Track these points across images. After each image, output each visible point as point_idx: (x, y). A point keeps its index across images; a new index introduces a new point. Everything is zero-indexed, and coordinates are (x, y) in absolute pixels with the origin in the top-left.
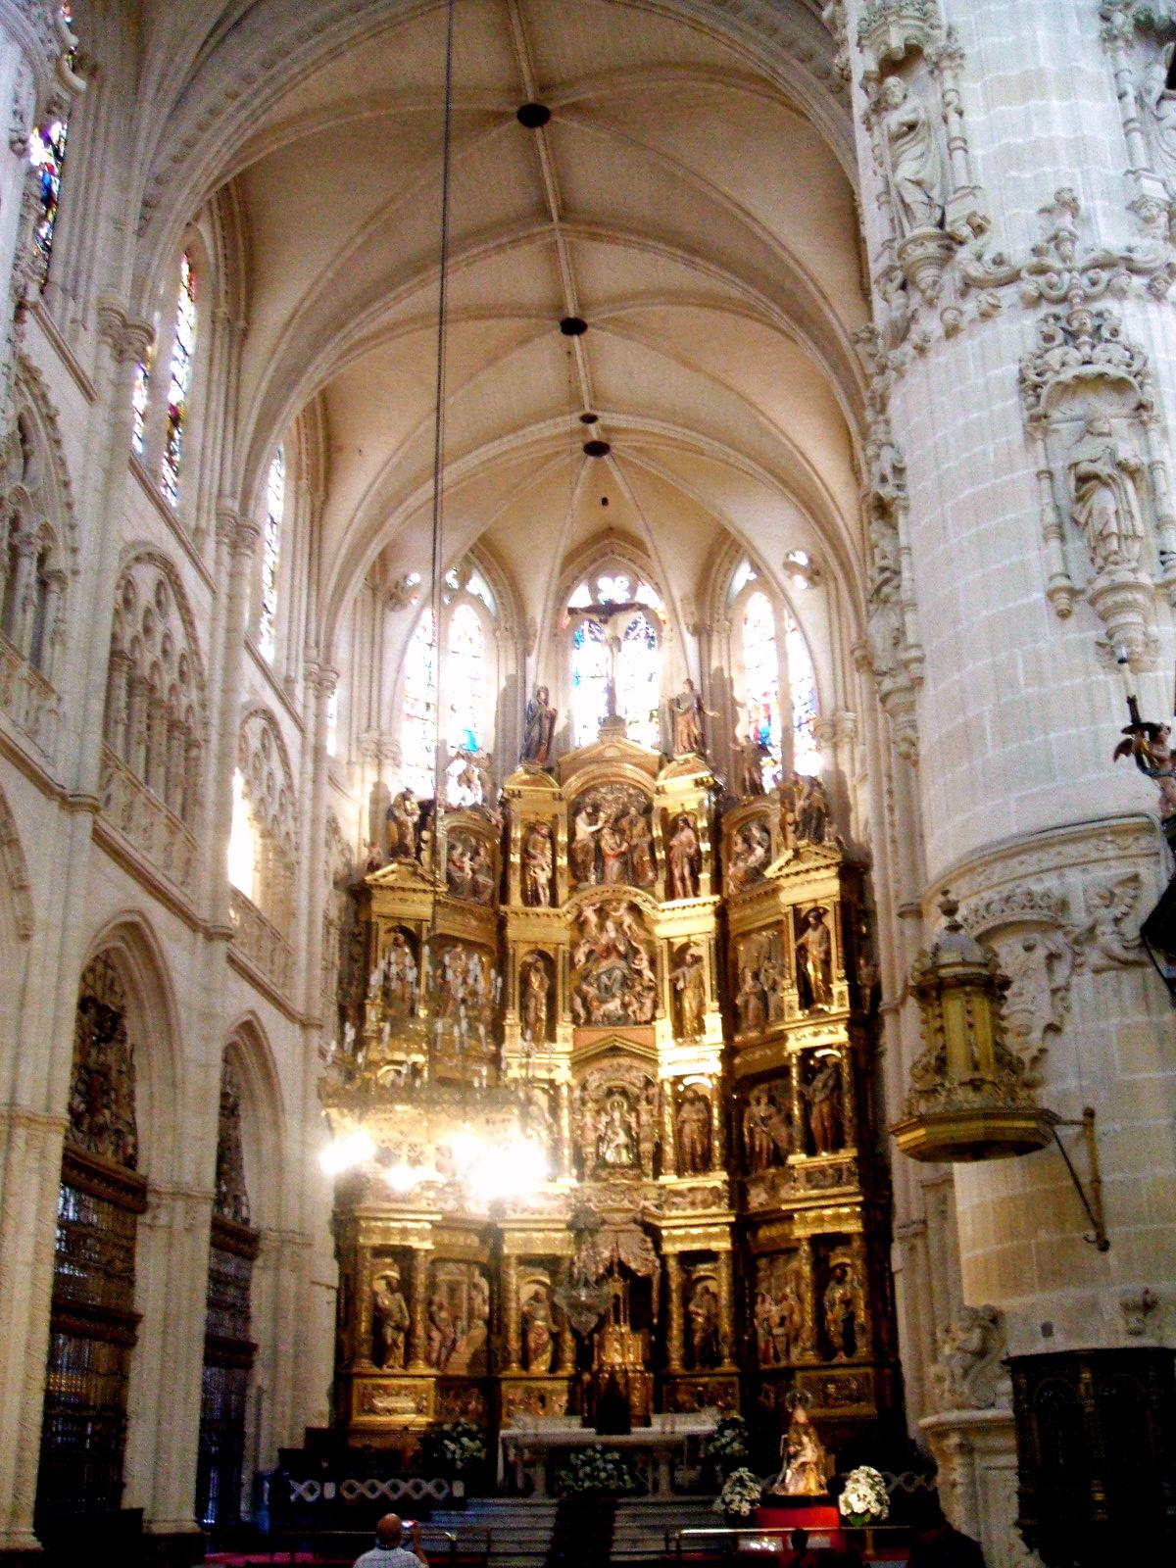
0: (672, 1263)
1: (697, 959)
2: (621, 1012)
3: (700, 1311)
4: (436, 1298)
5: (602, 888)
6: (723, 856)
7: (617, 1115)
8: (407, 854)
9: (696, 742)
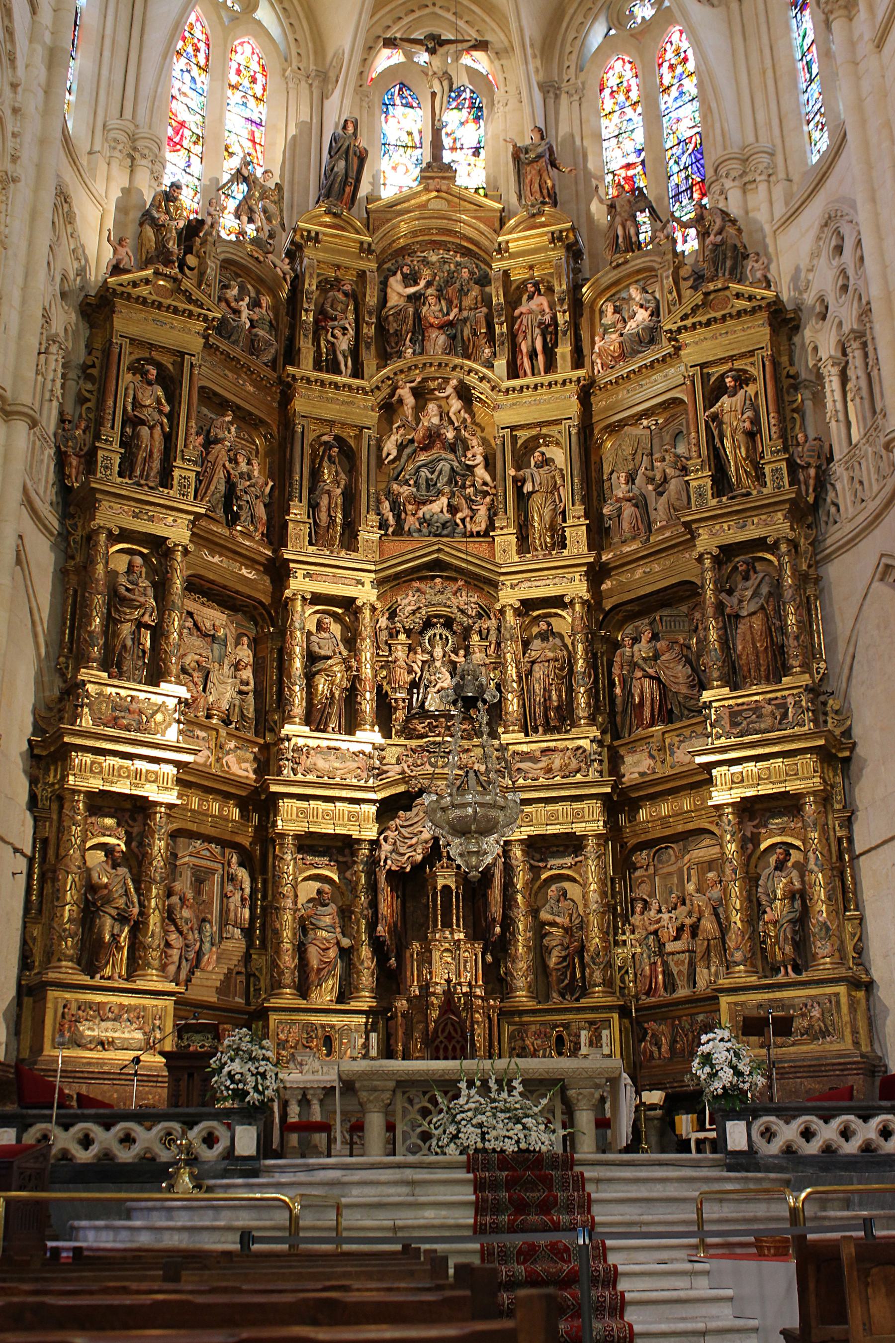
0: (517, 852)
1: (547, 462)
2: (448, 516)
3: (558, 920)
4: (178, 886)
5: (422, 359)
6: (585, 334)
7: (438, 652)
8: (168, 263)
9: (549, 196)
